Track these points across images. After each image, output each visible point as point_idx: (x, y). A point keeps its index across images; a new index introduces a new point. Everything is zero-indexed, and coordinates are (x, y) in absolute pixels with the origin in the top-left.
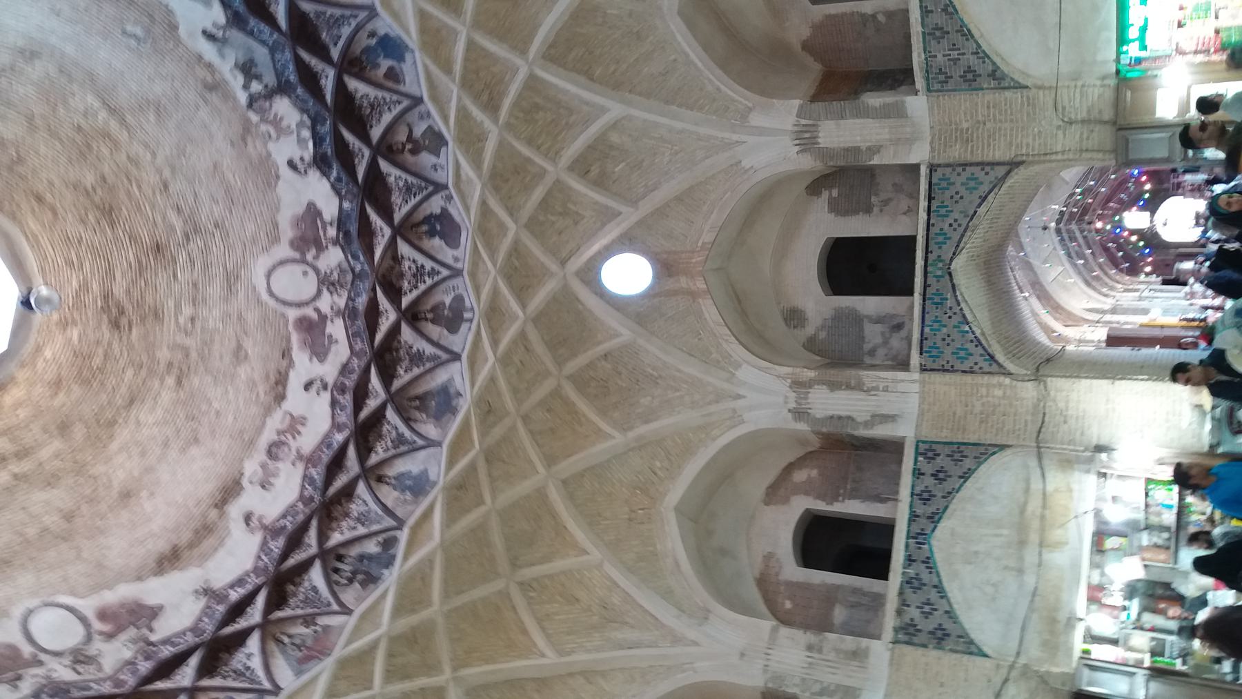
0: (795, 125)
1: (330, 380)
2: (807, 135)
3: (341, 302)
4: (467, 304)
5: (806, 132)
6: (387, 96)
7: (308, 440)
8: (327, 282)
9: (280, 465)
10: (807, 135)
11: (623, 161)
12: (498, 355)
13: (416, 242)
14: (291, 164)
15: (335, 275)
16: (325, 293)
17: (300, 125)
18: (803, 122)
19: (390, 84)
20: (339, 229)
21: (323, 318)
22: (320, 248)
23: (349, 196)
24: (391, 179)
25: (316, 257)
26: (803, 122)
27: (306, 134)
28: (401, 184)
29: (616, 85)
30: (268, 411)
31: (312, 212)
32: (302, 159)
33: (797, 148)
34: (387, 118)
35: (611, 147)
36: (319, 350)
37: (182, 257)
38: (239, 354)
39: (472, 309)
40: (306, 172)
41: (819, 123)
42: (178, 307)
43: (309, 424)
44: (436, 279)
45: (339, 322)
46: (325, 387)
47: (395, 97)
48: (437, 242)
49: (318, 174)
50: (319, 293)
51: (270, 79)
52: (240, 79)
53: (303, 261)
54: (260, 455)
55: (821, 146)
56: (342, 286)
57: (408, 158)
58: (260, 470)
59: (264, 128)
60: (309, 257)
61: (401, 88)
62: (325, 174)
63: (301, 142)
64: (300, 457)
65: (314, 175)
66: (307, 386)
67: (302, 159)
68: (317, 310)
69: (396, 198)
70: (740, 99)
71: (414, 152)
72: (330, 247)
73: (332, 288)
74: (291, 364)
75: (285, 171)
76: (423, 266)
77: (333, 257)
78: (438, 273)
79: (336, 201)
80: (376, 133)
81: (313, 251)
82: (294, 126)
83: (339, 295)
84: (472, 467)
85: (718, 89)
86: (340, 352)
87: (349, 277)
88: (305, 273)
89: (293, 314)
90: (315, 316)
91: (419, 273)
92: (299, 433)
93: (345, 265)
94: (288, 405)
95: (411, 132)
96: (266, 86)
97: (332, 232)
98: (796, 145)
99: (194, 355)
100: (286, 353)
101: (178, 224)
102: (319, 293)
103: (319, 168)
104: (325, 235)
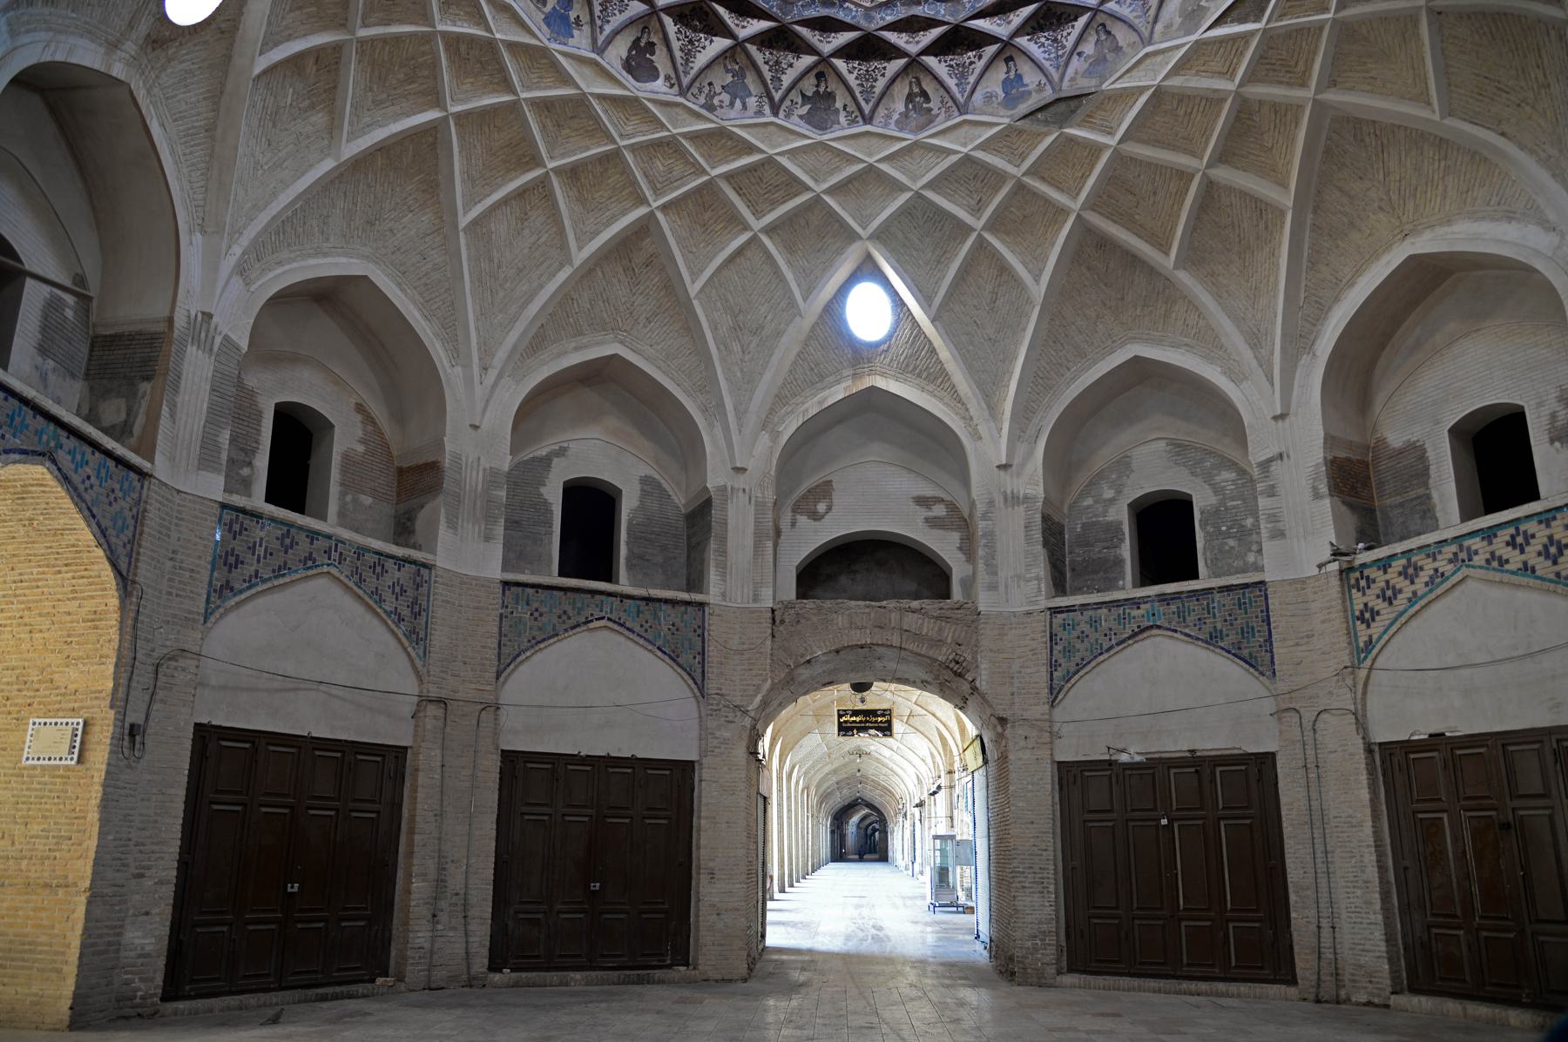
0: (216, 329)
2: (203, 335)
5: (207, 336)
10: (203, 335)
11: (291, 105)
18: (218, 340)
26: (218, 340)
29: (360, 164)
33: (193, 314)
35: (312, 107)
41: (213, 357)
55: (189, 347)
70: (260, 283)
85: (280, 263)
98: (196, 316)
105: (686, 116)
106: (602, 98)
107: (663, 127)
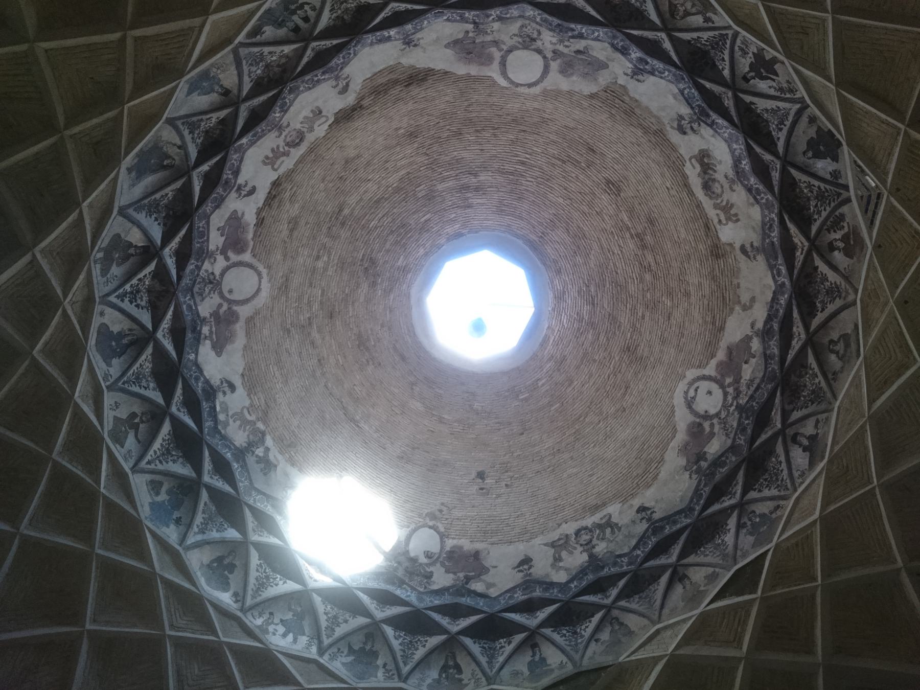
1: (233, 194)
3: (207, 266)
4: (98, 266)
6: (160, 467)
7: (270, 142)
8: (214, 283)
9: (298, 126)
12: (77, 211)
13: (135, 327)
14: (232, 387)
15: (207, 290)
16: (217, 273)
17: (226, 424)
19: (157, 478)
20: (200, 333)
21: (224, 252)
22: (215, 314)
23: (190, 364)
24: (152, 385)
25: (220, 306)
27: (221, 417)
28: (144, 383)
30: (290, 174)
31: (218, 348)
32: (224, 393)
34: (157, 445)
36: (235, 219)
37: (316, 306)
38: (294, 224)
39: (95, 262)
40: (222, 383)
42: (325, 269)
43: (262, 158)
44: (121, 291)
45: (212, 247)
46: (239, 188)
47: (152, 466)
48: (115, 329)
49: (212, 382)
50: (223, 273)
51: (251, 460)
52: (271, 457)
53: (230, 302)
54: (310, 138)
56: (204, 279)
57: (137, 408)
58: (316, 126)
59: (252, 418)
60: (225, 307)
61: (148, 477)
62: (207, 382)
63: (225, 410)
64: (280, 129)
65: (215, 381)
66: (253, 191)
67: (224, 393)
68: (227, 259)
69: (148, 367)
71: (133, 415)
72: (208, 316)
73: (212, 277)
74: (259, 211)
75: (237, 382)
76: (131, 302)
77: (205, 308)
78: (118, 297)
79: (200, 359)
80: (166, 428)
81: (222, 311)
82: (231, 421)
83: (207, 271)
84: (139, 90)
86: (218, 219)
87: (196, 289)
88: (230, 291)
89: (247, 257)
90: (230, 254)
91: (133, 296)
92: (273, 150)
93: (198, 299)
94: (274, 176)
95: (136, 436)
96: (253, 452)
97: (205, 330)
99: (324, 230)
100: (260, 222)
101: (315, 334)
102: (223, 273)
103: (211, 387)
104: (211, 328)
105: (239, 629)
106: (168, 584)
107: (214, 632)
